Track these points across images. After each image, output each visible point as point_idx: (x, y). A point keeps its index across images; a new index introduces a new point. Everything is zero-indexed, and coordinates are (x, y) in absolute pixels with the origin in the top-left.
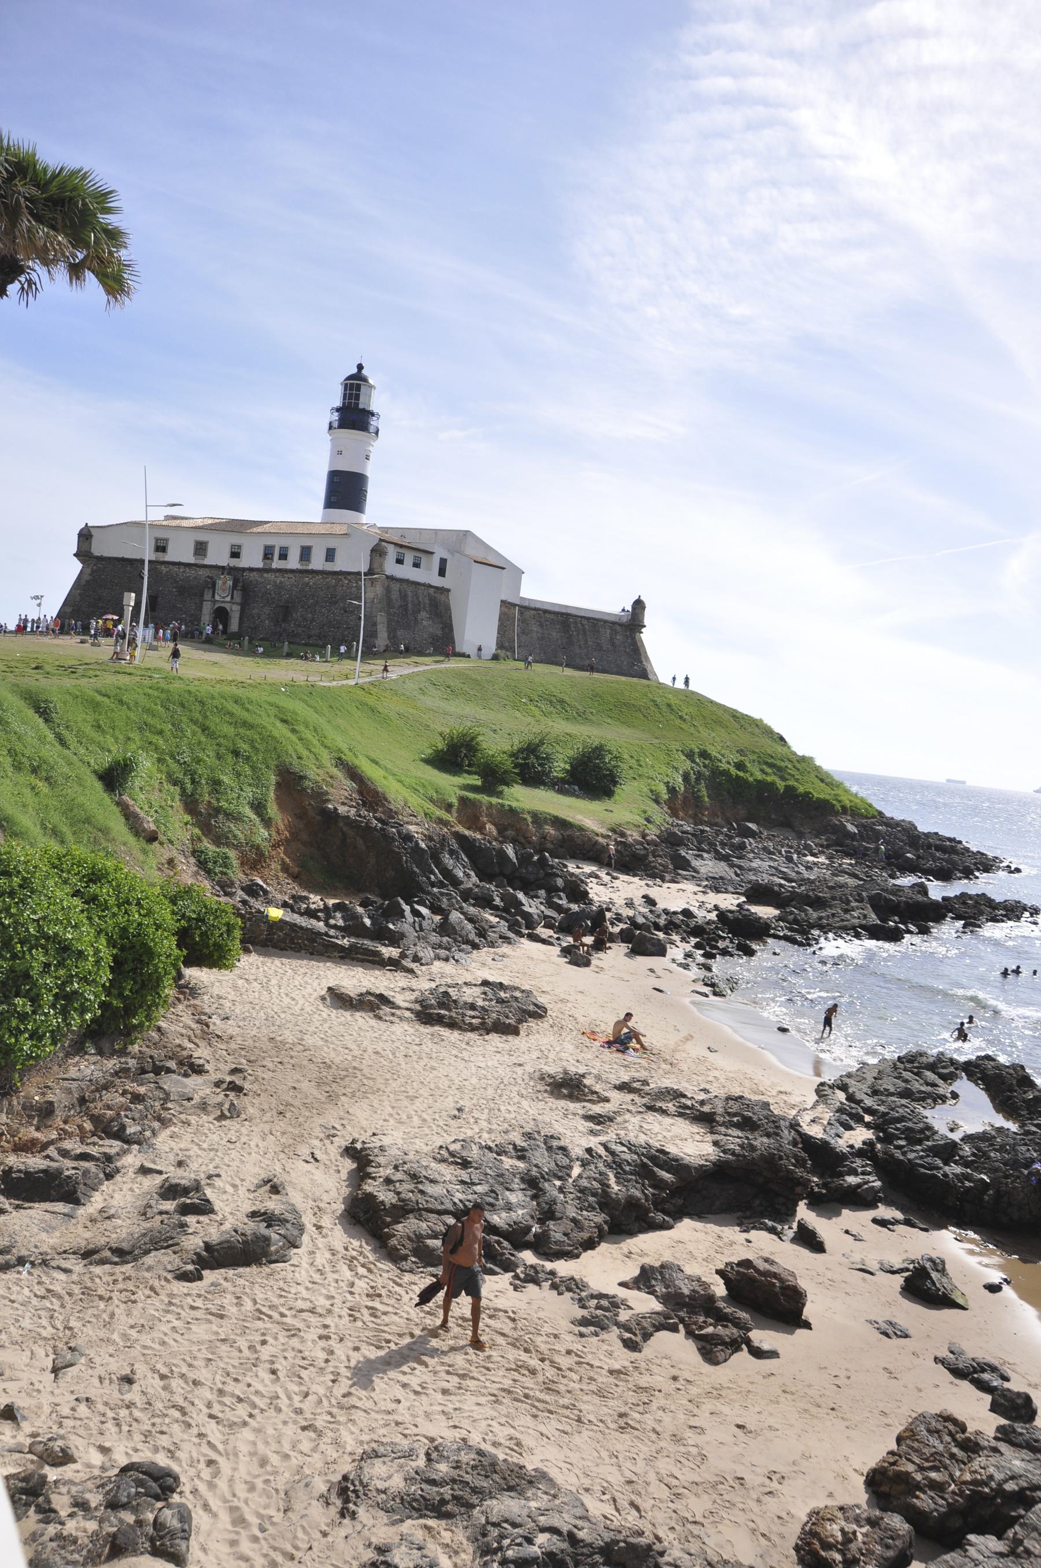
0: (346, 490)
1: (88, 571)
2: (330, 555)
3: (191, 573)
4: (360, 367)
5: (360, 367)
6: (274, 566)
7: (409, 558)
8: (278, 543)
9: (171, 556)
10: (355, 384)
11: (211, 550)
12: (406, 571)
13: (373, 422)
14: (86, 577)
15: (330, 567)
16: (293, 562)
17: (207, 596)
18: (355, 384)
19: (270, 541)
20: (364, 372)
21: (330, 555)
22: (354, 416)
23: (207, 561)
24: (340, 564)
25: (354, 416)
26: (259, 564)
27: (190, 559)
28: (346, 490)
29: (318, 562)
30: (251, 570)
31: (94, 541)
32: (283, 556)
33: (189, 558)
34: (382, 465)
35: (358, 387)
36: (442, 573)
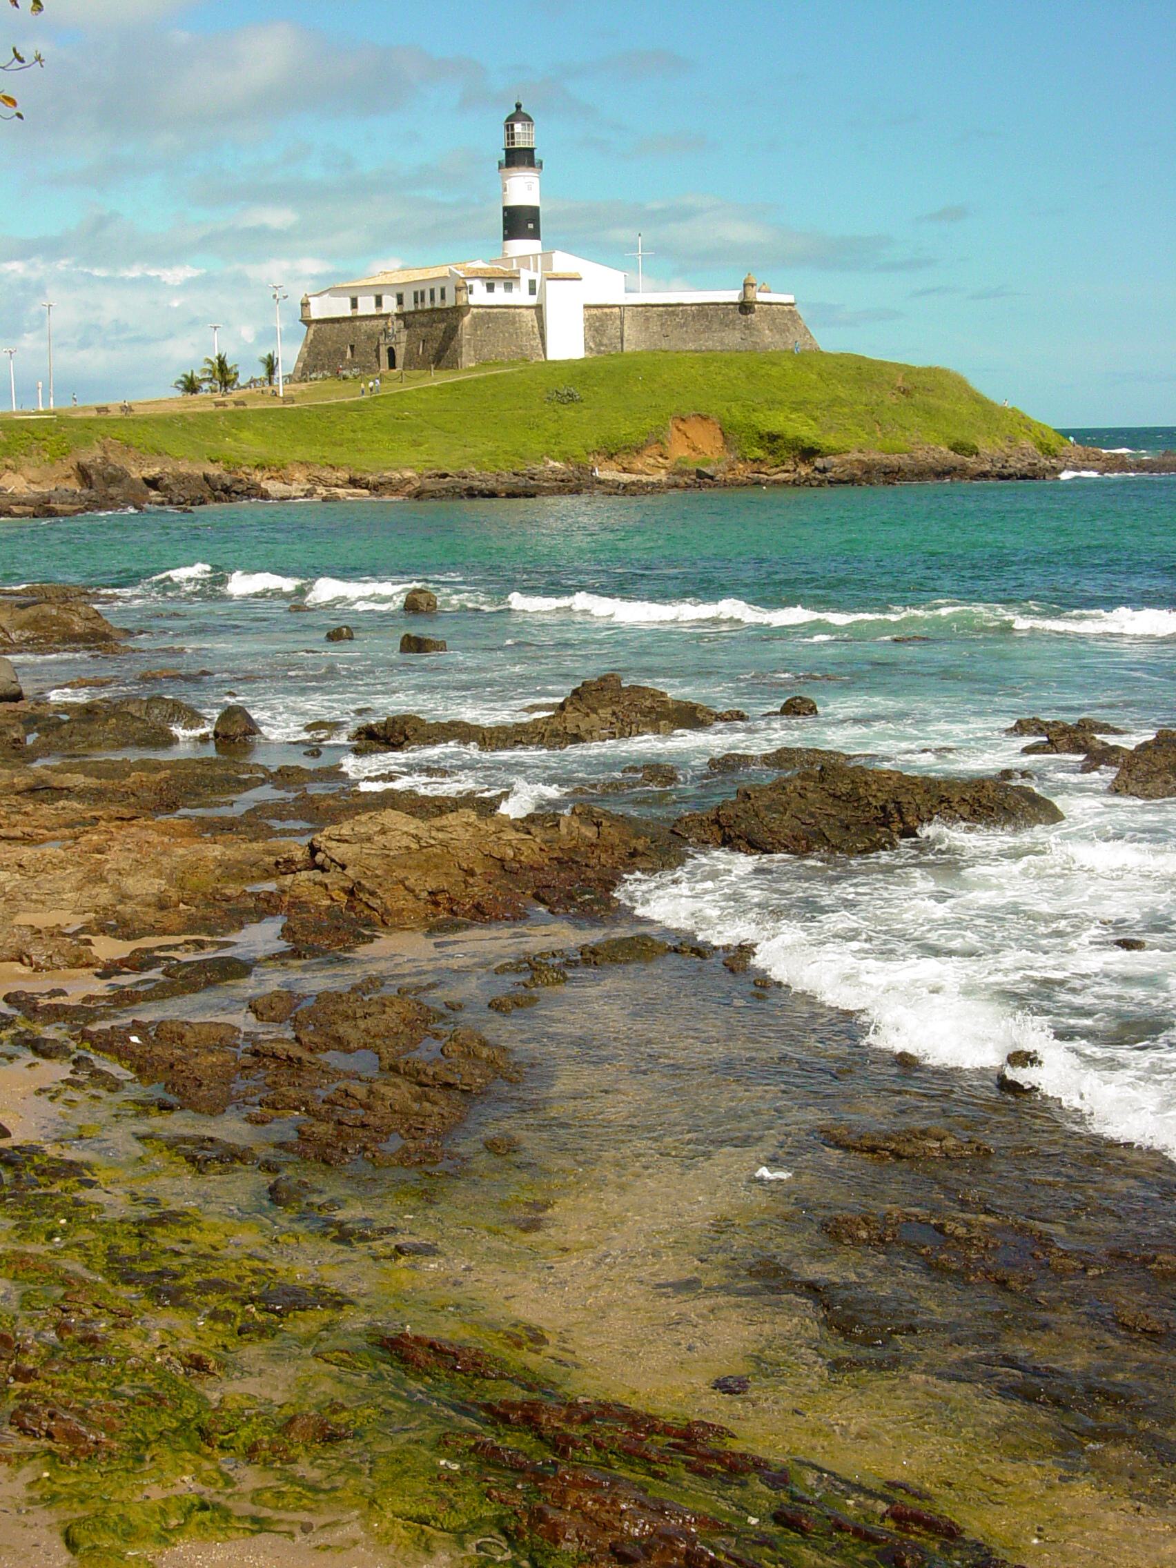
1: (311, 331)
4: (518, 106)
5: (518, 106)
6: (420, 307)
7: (499, 289)
8: (419, 289)
9: (361, 312)
12: (500, 296)
13: (537, 155)
14: (311, 337)
16: (428, 305)
20: (523, 110)
23: (384, 311)
26: (412, 309)
27: (373, 311)
29: (438, 304)
31: (311, 306)
32: (423, 300)
35: (512, 126)
36: (532, 291)
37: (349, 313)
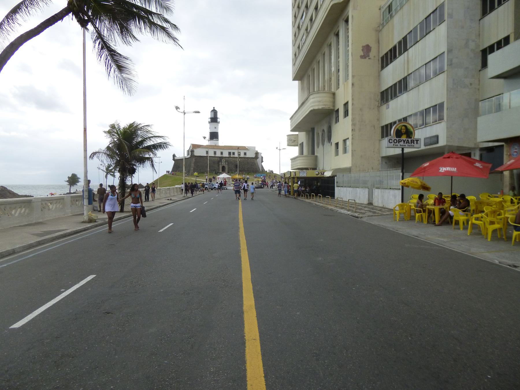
0: (214, 136)
2: (245, 154)
3: (214, 158)
10: (214, 112)
11: (209, 152)
15: (245, 156)
16: (236, 155)
17: (220, 163)
18: (214, 112)
19: (230, 151)
21: (245, 154)
22: (214, 119)
24: (248, 155)
25: (214, 119)
28: (214, 136)
29: (242, 155)
30: (226, 157)
33: (213, 155)
34: (221, 130)
37: (206, 155)
